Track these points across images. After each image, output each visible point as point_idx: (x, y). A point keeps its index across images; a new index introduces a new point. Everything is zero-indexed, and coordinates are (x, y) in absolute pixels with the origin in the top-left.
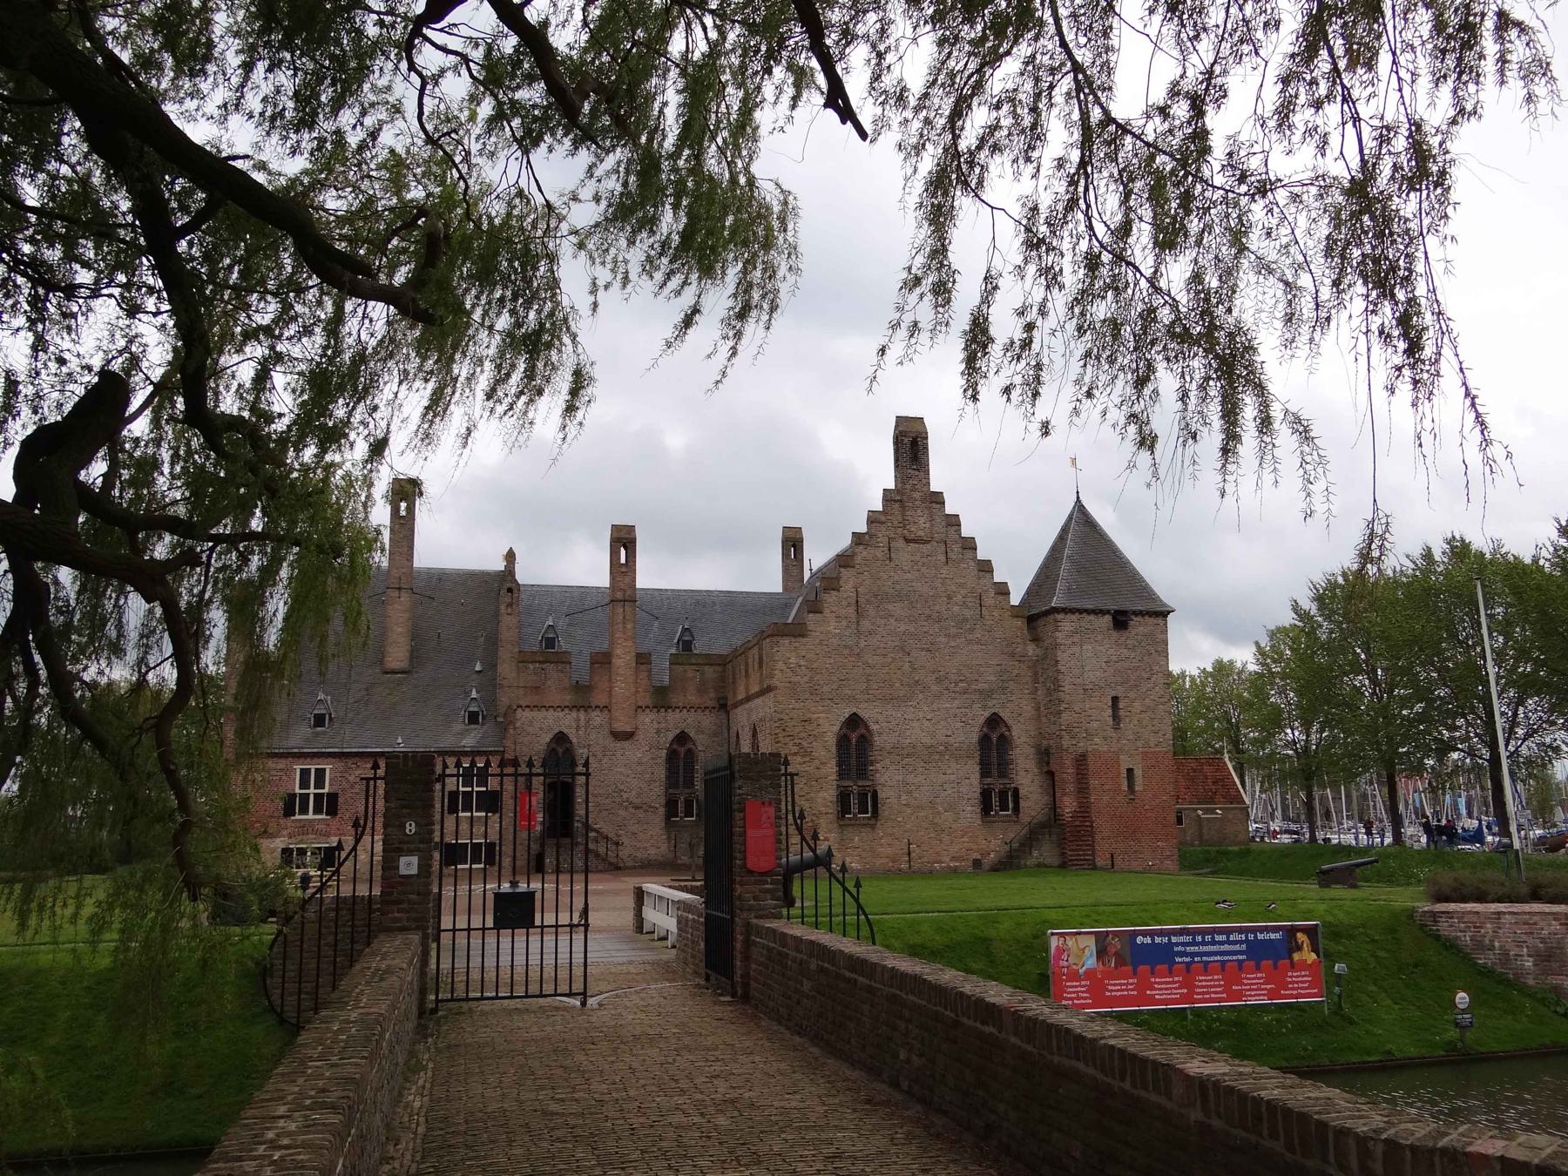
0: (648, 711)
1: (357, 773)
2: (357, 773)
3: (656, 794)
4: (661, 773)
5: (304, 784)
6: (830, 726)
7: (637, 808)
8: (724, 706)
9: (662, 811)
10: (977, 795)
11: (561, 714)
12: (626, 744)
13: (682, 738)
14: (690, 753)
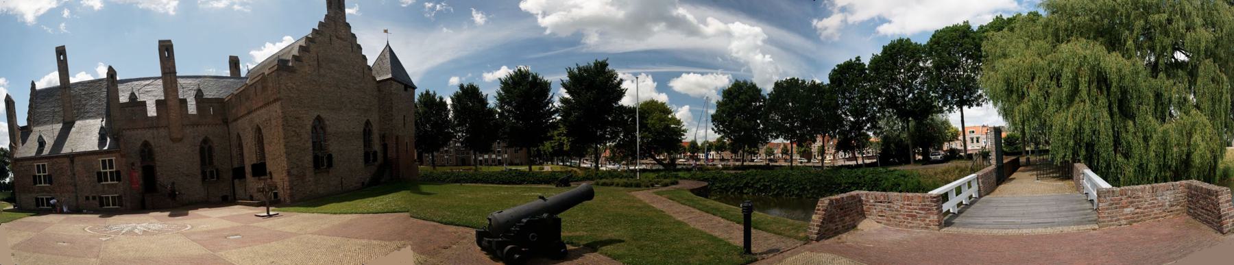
0: (188, 127)
1: (57, 165)
2: (57, 165)
3: (196, 168)
4: (197, 158)
5: (39, 172)
7: (187, 176)
8: (226, 122)
9: (200, 177)
10: (363, 155)
11: (145, 132)
13: (205, 141)
14: (210, 148)
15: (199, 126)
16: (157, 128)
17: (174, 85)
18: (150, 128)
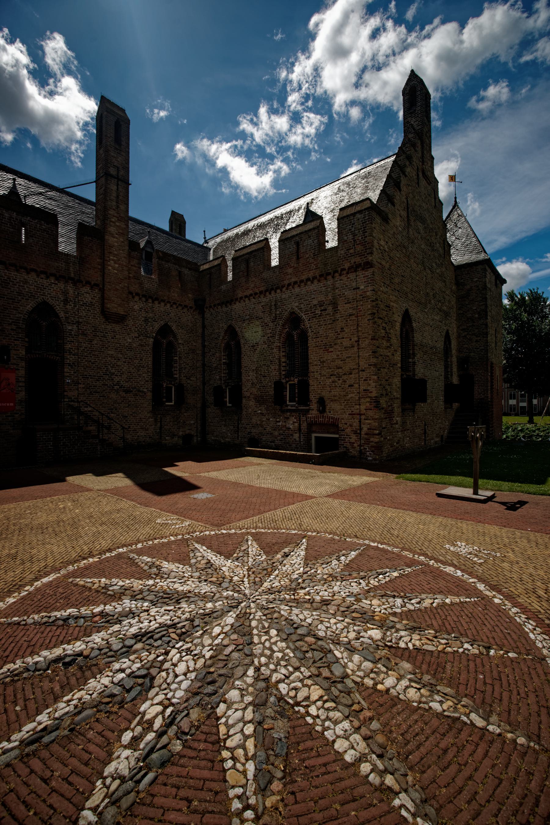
0: (137, 298)
6: (398, 319)
7: (127, 391)
9: (149, 395)
10: (443, 388)
12: (117, 327)
13: (165, 330)
15: (156, 302)
16: (76, 282)
17: (122, 207)
18: (59, 278)
